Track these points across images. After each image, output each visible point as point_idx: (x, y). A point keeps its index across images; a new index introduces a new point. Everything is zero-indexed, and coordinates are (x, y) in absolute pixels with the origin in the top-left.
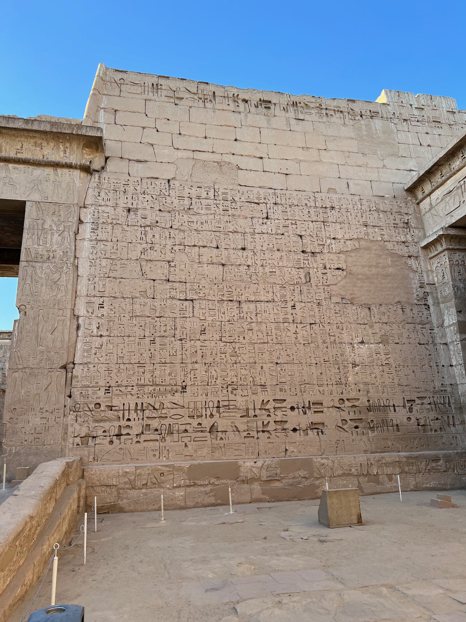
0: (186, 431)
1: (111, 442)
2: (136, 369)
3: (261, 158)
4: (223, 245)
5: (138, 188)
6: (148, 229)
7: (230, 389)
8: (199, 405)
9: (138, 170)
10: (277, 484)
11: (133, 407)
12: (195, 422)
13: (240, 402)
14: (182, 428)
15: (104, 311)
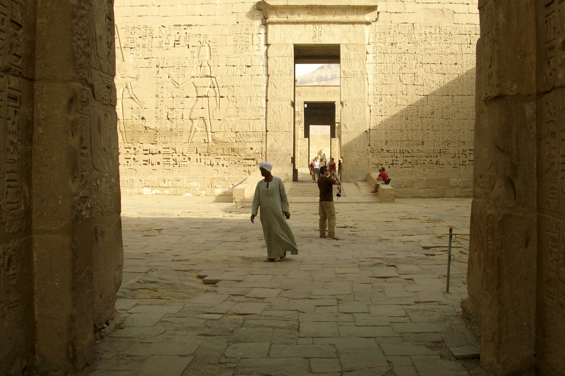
0: (424, 163)
1: (389, 167)
2: (399, 133)
3: (468, 4)
4: (444, 62)
5: (396, 30)
6: (402, 55)
7: (446, 143)
8: (431, 151)
9: (396, 19)
10: (468, 189)
11: (398, 151)
12: (428, 159)
13: (451, 150)
14: (422, 162)
15: (383, 102)
